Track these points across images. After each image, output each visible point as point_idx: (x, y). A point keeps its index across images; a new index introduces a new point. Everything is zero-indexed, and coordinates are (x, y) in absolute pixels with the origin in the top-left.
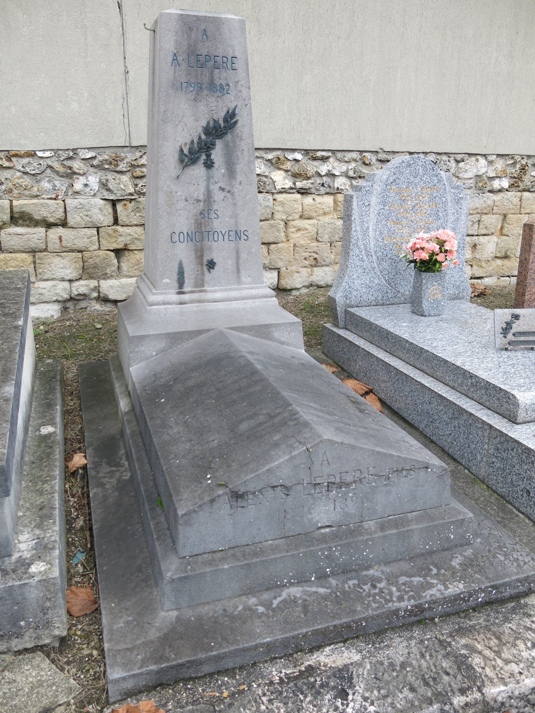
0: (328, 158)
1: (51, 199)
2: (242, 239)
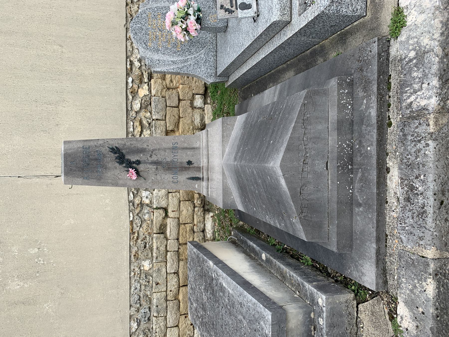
0: (131, 61)
1: (153, 215)
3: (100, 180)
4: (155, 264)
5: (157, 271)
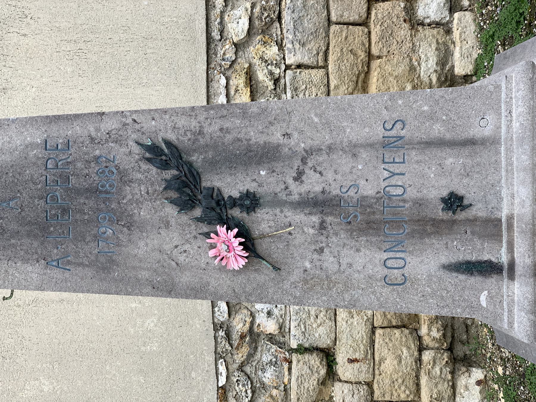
1: (290, 369)
2: (403, 133)
3: (110, 274)
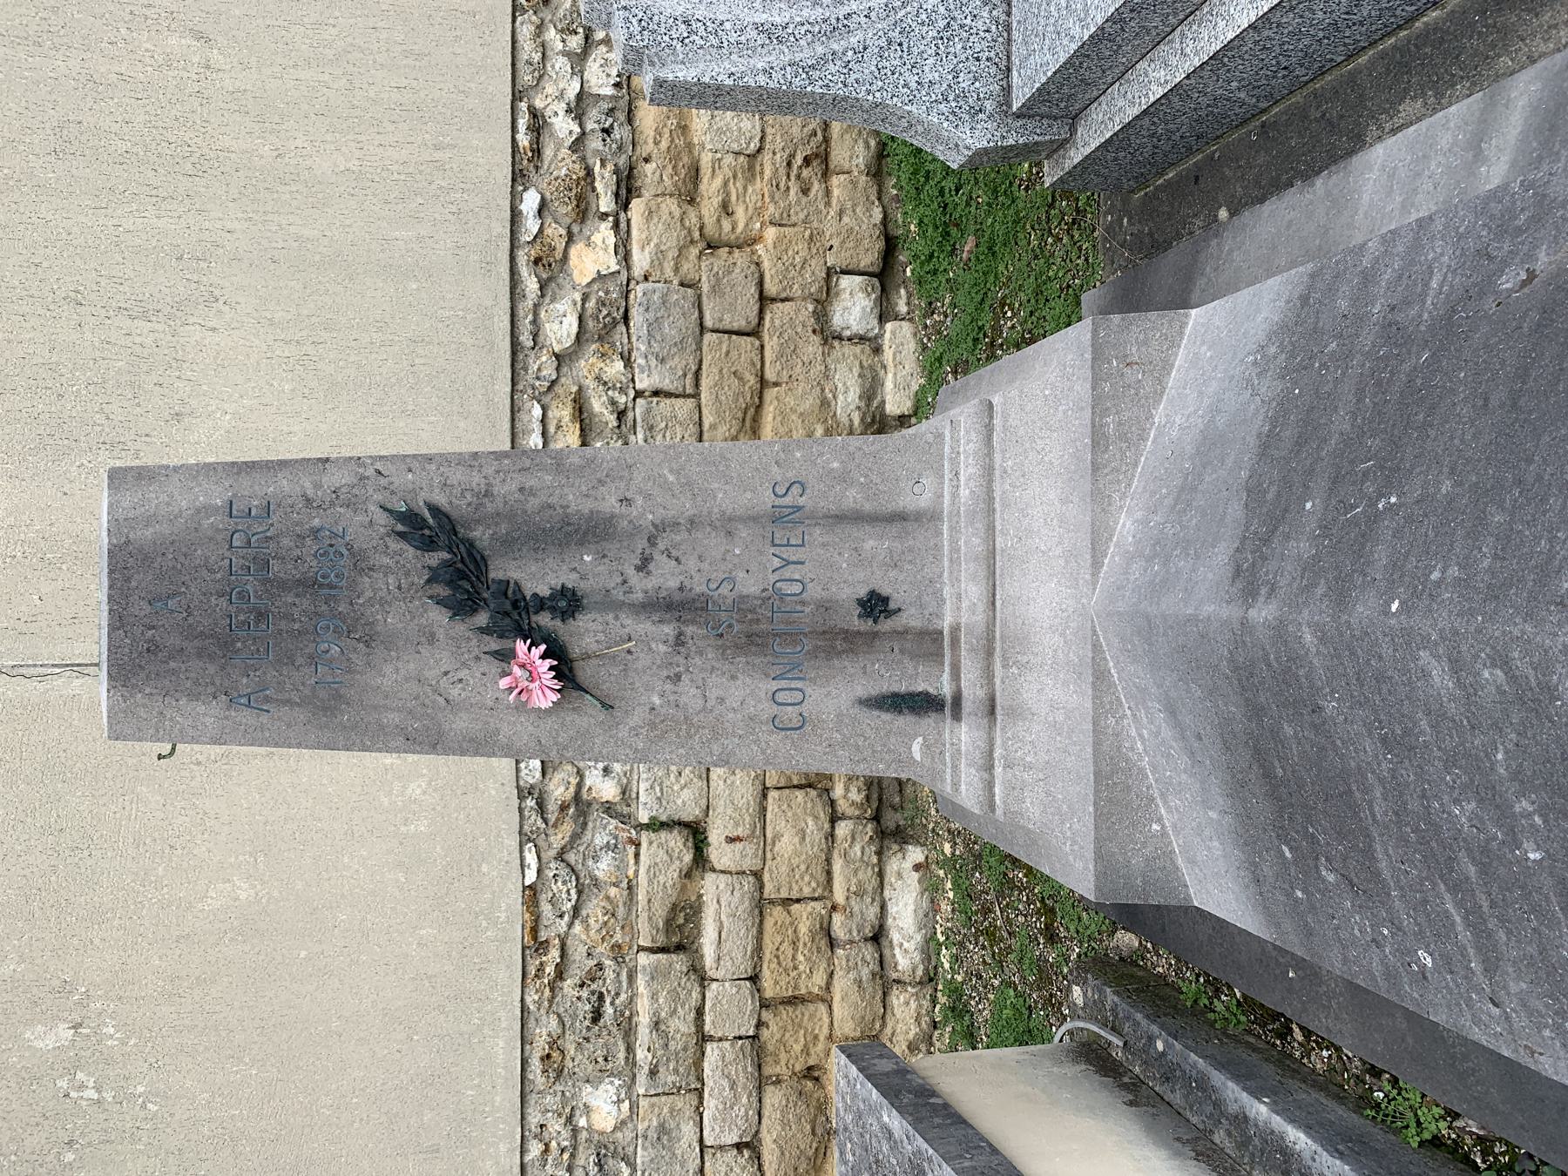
0: (534, 113)
1: (637, 855)
2: (801, 501)
3: (335, 717)
4: (643, 1103)
5: (652, 1135)
